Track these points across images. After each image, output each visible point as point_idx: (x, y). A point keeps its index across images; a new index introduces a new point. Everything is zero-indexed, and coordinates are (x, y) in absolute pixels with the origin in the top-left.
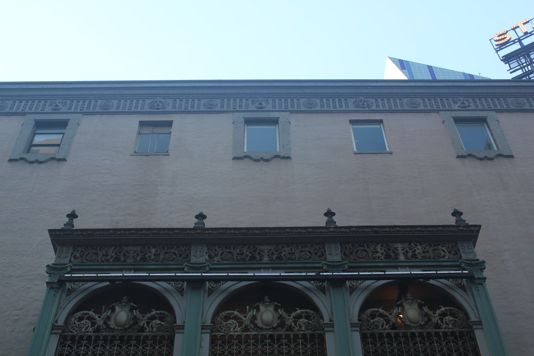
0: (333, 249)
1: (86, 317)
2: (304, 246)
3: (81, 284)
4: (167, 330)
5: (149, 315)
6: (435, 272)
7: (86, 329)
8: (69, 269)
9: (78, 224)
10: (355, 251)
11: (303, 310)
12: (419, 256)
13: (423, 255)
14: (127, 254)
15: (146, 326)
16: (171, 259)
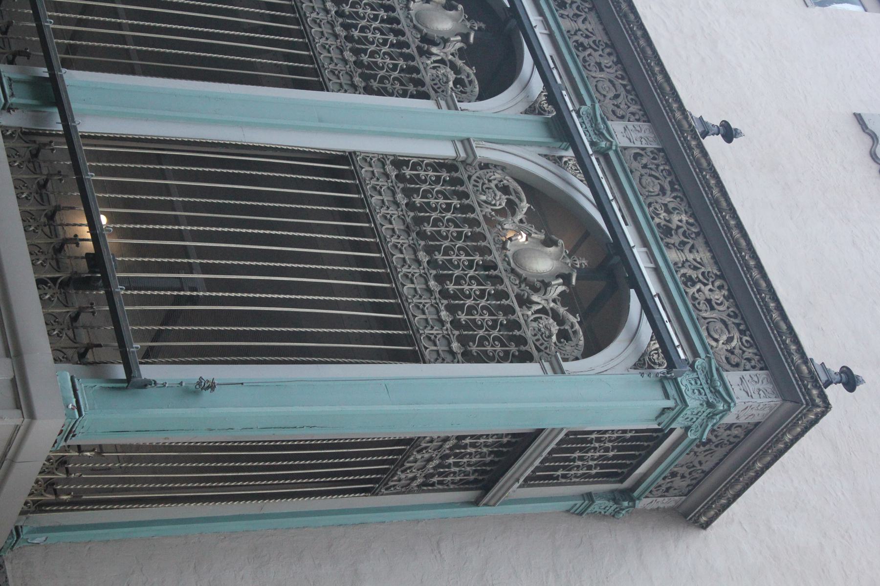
0: (758, 386)
1: (511, 197)
2: (628, 88)
3: (581, 176)
4: (542, 348)
5: (562, 310)
6: (611, 197)
7: (485, 202)
8: (603, 144)
9: (713, 144)
10: (654, 173)
11: (577, 327)
12: (694, 290)
13: (701, 297)
14: (688, 247)
15: (434, 58)
16: (713, 333)
